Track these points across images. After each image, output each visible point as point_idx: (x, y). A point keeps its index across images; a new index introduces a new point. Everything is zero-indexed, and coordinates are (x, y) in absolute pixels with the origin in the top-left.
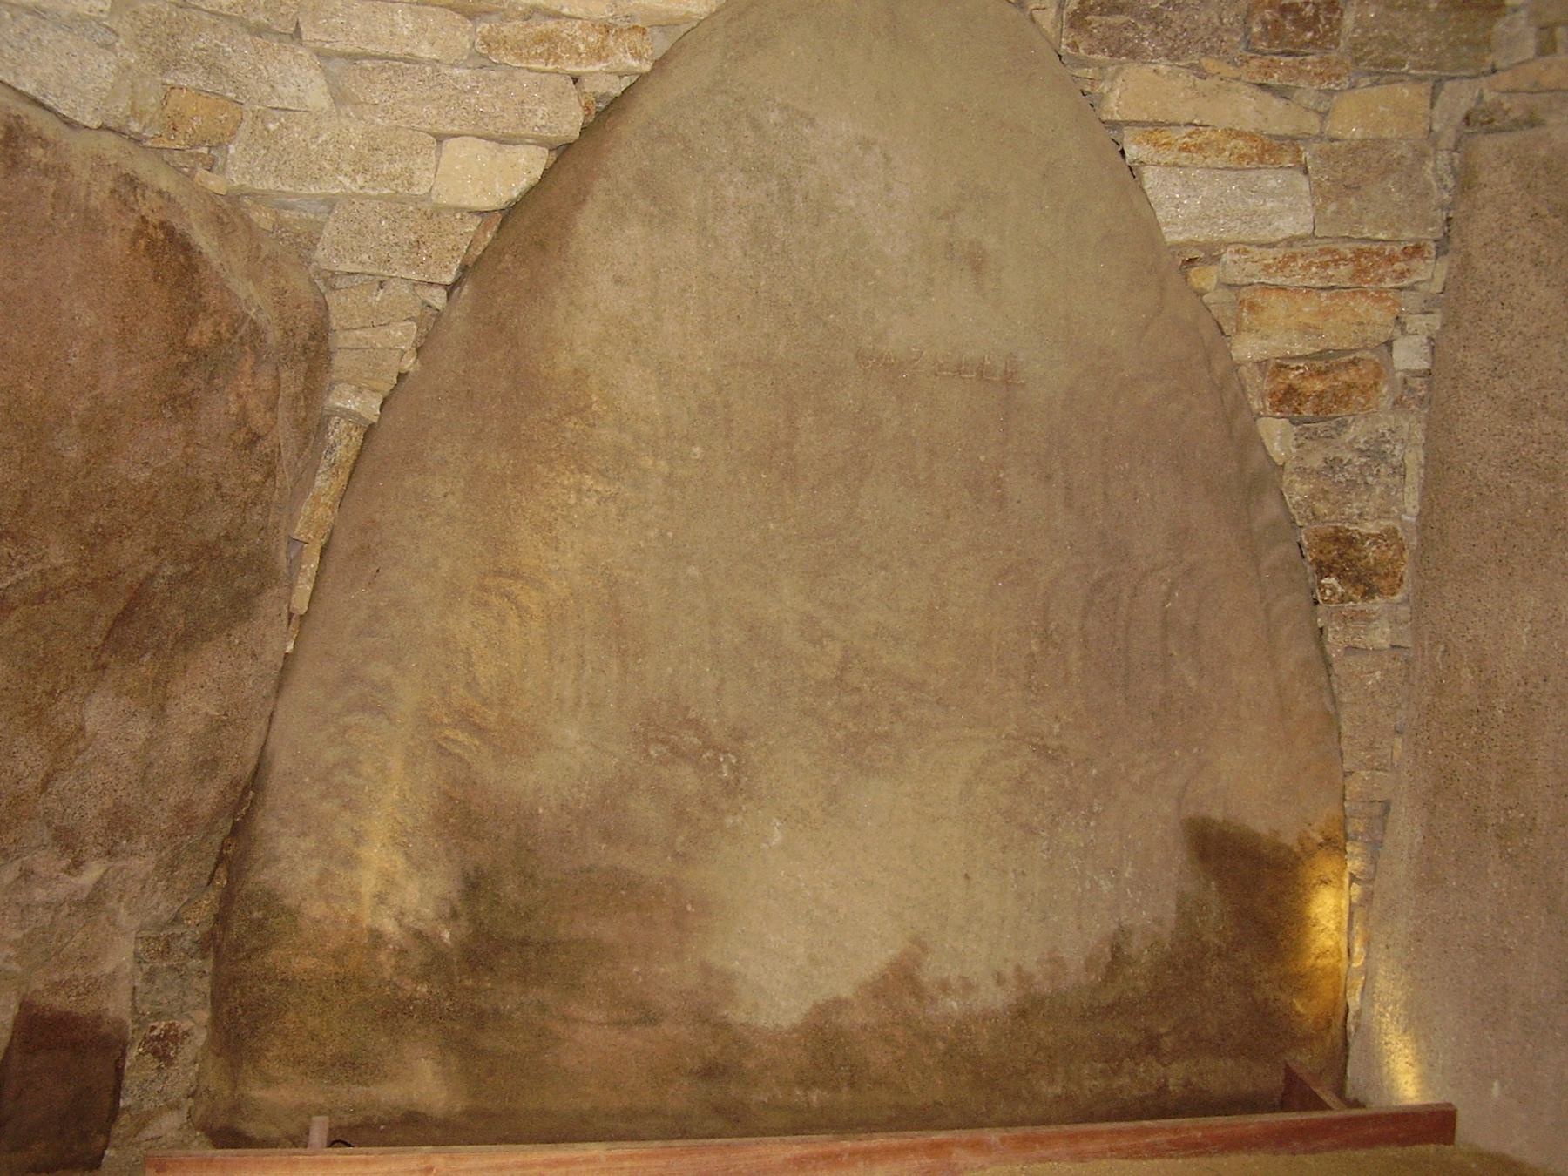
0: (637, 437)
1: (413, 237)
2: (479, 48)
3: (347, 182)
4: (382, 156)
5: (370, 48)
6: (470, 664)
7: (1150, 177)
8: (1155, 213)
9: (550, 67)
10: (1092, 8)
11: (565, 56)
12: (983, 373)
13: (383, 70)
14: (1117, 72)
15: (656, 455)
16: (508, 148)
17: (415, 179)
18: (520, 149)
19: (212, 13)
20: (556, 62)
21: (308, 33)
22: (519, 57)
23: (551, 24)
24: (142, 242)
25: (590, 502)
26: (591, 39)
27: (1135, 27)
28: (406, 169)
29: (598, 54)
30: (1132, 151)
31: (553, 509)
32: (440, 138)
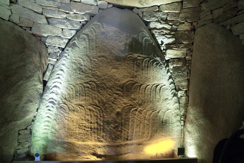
5: (52, 17)
6: (65, 96)
9: (76, 20)
16: (71, 30)
23: (77, 14)
24: (15, 37)
29: (83, 18)
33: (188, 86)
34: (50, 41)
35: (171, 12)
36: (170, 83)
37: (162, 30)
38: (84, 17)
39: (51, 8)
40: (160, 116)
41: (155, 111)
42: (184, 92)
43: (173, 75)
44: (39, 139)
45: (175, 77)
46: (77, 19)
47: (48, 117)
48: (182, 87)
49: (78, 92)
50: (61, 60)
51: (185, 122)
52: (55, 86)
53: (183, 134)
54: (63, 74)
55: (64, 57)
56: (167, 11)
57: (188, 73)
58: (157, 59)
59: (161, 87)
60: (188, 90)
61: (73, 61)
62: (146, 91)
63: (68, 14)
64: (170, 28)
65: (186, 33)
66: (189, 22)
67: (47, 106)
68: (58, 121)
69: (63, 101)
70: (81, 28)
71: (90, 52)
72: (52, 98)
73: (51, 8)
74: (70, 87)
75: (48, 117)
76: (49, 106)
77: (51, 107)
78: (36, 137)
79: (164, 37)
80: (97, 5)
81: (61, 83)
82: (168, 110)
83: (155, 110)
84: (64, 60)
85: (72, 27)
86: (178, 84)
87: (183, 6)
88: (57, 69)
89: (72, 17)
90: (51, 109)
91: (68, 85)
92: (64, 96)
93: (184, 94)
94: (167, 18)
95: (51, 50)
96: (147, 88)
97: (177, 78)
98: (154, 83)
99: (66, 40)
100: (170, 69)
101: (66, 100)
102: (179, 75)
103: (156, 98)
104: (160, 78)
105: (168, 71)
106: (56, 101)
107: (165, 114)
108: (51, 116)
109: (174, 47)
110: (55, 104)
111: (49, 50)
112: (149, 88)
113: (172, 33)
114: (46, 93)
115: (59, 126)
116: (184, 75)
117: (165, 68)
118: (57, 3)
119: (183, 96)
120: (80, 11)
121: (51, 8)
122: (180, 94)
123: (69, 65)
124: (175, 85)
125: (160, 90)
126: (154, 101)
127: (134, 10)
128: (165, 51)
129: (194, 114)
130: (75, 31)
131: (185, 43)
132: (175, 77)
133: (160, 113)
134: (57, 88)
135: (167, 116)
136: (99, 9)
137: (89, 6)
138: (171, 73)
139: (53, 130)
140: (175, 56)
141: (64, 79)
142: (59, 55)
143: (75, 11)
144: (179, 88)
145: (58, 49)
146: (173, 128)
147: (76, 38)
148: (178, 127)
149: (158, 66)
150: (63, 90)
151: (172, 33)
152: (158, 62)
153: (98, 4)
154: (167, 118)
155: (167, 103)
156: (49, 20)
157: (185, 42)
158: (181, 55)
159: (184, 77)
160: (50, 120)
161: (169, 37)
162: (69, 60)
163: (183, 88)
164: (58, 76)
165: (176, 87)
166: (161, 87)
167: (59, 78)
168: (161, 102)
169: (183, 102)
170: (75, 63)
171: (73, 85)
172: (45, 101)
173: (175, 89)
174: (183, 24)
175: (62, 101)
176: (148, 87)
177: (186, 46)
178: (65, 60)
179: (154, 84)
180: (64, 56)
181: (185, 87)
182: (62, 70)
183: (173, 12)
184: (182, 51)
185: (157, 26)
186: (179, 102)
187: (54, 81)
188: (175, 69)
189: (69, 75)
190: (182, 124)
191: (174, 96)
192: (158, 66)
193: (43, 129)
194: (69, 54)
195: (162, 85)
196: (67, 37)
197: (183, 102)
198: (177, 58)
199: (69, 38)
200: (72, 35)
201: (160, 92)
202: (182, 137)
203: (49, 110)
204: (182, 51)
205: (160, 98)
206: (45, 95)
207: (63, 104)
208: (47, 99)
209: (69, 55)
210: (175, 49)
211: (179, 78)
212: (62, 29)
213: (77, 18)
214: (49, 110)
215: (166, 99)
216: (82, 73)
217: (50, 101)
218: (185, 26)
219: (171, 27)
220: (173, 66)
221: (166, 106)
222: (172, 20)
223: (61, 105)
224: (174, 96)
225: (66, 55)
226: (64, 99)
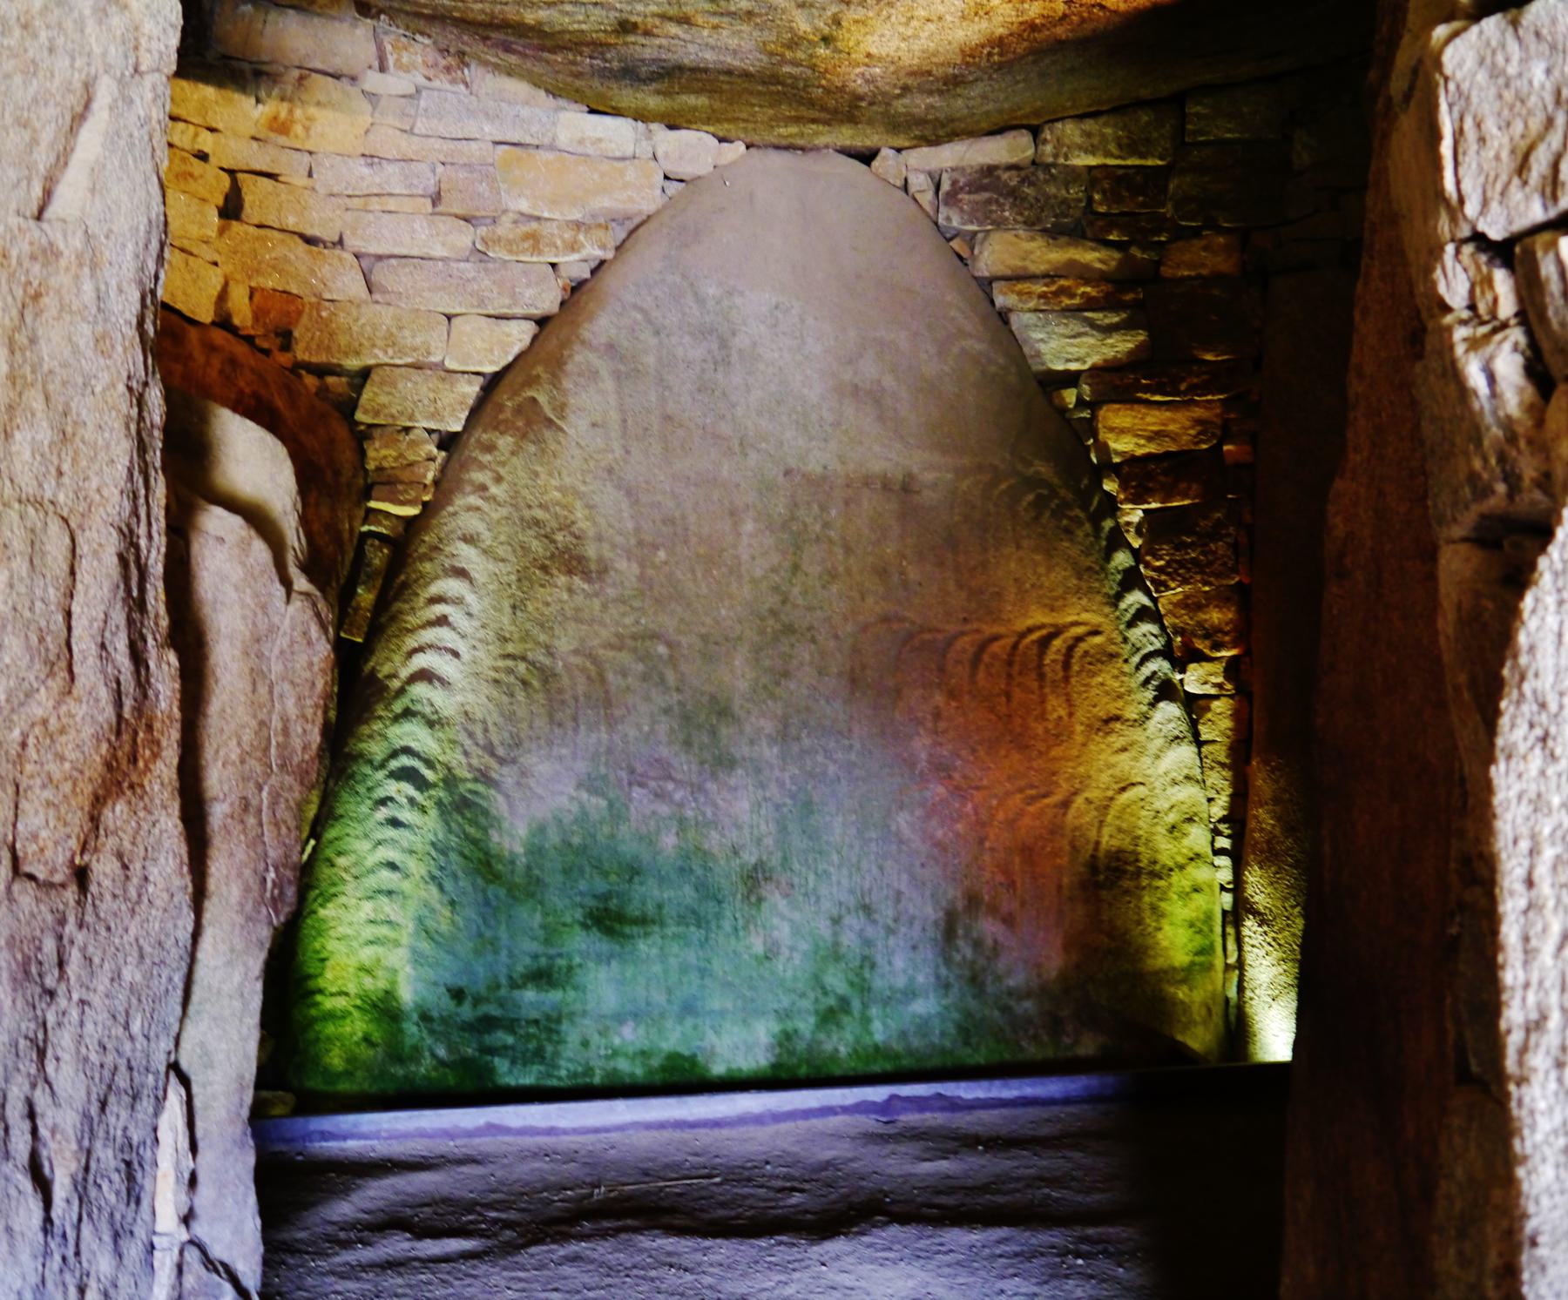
0: (614, 546)
1: (432, 395)
2: (479, 247)
3: (381, 354)
4: (407, 333)
5: (397, 251)
6: (486, 730)
7: (1016, 321)
8: (1020, 348)
9: (535, 259)
10: (962, 189)
12: (886, 486)
14: (985, 239)
15: (629, 559)
17: (433, 349)
18: (513, 323)
19: (282, 231)
21: (347, 241)
22: (510, 252)
23: (534, 225)
25: (579, 599)
26: (566, 236)
27: (997, 202)
28: (423, 343)
29: (573, 247)
30: (1000, 301)
31: (547, 604)
33: (1242, 634)
34: (383, 399)
35: (1111, 162)
36: (1128, 616)
37: (1063, 282)
38: (581, 237)
40: (1076, 829)
41: (1045, 796)
42: (1218, 667)
43: (1147, 565)
44: (340, 1003)
45: (1163, 577)
46: (540, 253)
47: (392, 866)
48: (1207, 636)
49: (563, 702)
50: (450, 509)
51: (1238, 859)
52: (425, 675)
53: (1231, 946)
54: (470, 598)
55: (468, 489)
56: (1092, 161)
57: (1235, 546)
58: (1038, 473)
59: (1070, 649)
60: (1247, 653)
61: (527, 513)
62: (981, 675)
64: (1113, 263)
65: (1216, 292)
66: (1228, 231)
67: (383, 802)
68: (448, 885)
69: (475, 762)
70: (562, 303)
71: (628, 452)
72: (407, 751)
73: (391, 204)
74: (510, 671)
75: (392, 866)
76: (391, 799)
77: (407, 806)
78: (319, 998)
79: (1075, 326)
80: (655, 158)
81: (456, 654)
82: (1123, 789)
83: (1043, 790)
84: (470, 508)
85: (507, 302)
86: (1186, 620)
87: (1189, 127)
88: (427, 567)
89: (510, 242)
90: (406, 815)
91: (501, 663)
92: (478, 730)
93: (1220, 680)
94: (1090, 200)
95: (384, 452)
96: (986, 658)
97: (1173, 585)
98: (1030, 622)
99: (470, 383)
100: (1128, 524)
101: (493, 754)
102: (1181, 564)
103: (1042, 717)
104: (1060, 591)
105: (1117, 540)
106: (429, 764)
107: (1109, 819)
108: (412, 864)
109: (1146, 389)
110: (434, 786)
111: (371, 453)
112: (994, 656)
113: (1129, 297)
114: (366, 722)
115: (457, 918)
116: (1210, 563)
117: (1088, 527)
118: (423, 168)
119: (1216, 697)
120: (554, 202)
121: (391, 204)
122: (1195, 680)
123: (503, 538)
124: (1163, 628)
125: (1067, 665)
126: (1035, 737)
127: (875, 164)
128: (1086, 414)
129: (1276, 800)
130: (530, 328)
131: (1209, 357)
132: (1163, 577)
133: (1075, 805)
134: (437, 683)
135: (1124, 825)
136: (666, 177)
137: (605, 166)
138: (1135, 553)
139: (425, 946)
140: (1150, 439)
141: (477, 624)
142: (430, 476)
143: (524, 206)
144: (1187, 645)
145: (424, 442)
146: (1163, 904)
147: (539, 370)
148: (1195, 896)
149: (1047, 514)
150: (471, 697)
151: (1129, 297)
152: (1045, 492)
153: (660, 154)
154: (1126, 843)
155: (1118, 745)
156: (380, 274)
157: (1208, 351)
158: (1192, 432)
159: (1218, 576)
160: (406, 886)
161: (1107, 321)
162: (504, 512)
163: (1217, 646)
164: (440, 609)
165: (1169, 642)
166: (1070, 649)
167: (442, 621)
168: (1079, 739)
169: (1223, 733)
170: (537, 523)
171: (533, 664)
172: (367, 770)
173: (1166, 653)
174: (1195, 242)
175: (470, 765)
176: (995, 647)
177: (1215, 379)
178: (478, 509)
179: (1030, 630)
180: (471, 482)
181: (1227, 638)
182: (461, 573)
183: (1129, 162)
184: (1198, 412)
185: (1033, 257)
186: (1196, 735)
187: (411, 642)
188: (1154, 525)
189: (506, 604)
190: (1225, 875)
191: (1157, 699)
192: (1047, 514)
193: (361, 940)
194: (502, 471)
195: (1080, 630)
196: (480, 363)
197: (1223, 733)
198: (1167, 454)
199: (490, 369)
200: (507, 353)
201: (1066, 679)
202: (1232, 960)
203: (395, 823)
204: (1198, 412)
205: (1071, 715)
206: (365, 729)
207: (476, 780)
208: (378, 758)
209: (499, 479)
210: (1147, 396)
211: (1185, 582)
212: (449, 317)
213: (535, 241)
214: (395, 823)
215: (1107, 721)
216: (586, 586)
217: (394, 764)
218: (1205, 248)
219: (1117, 255)
220: (1146, 506)
221: (1113, 766)
222: (1123, 214)
223: (462, 788)
224: (1157, 699)
225: (479, 477)
226: (484, 748)
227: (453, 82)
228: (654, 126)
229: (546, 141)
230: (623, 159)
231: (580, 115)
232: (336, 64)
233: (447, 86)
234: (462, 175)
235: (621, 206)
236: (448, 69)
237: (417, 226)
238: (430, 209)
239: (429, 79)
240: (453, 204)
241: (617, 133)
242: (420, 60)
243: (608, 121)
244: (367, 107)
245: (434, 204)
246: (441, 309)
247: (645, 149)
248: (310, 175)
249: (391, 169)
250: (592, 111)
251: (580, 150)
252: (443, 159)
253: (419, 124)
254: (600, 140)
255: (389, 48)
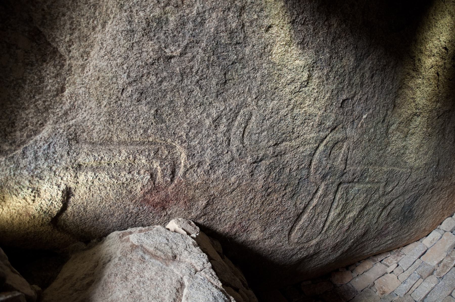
9: (450, 269)
11: (449, 265)
13: (431, 294)
20: (449, 267)
22: (444, 272)
23: (442, 263)
32: (450, 295)
38: (452, 257)
39: (415, 285)
63: (435, 273)
80: (445, 231)
121: (416, 286)
136: (452, 232)
137: (440, 241)
143: (436, 263)
153: (445, 230)
212: (450, 295)
227: (401, 256)
228: (438, 227)
229: (426, 249)
230: (441, 238)
231: (426, 239)
232: (381, 273)
233: (401, 258)
234: (420, 269)
235: (451, 245)
236: (398, 255)
237: (424, 285)
238: (423, 280)
239: (396, 260)
240: (425, 275)
241: (435, 234)
242: (392, 259)
243: (430, 235)
244: (392, 274)
245: (422, 278)
246: (447, 295)
247: (442, 231)
248: (397, 295)
249: (408, 280)
250: (427, 236)
251: (433, 244)
252: (414, 270)
253: (404, 269)
254: (434, 239)
255: (385, 262)
